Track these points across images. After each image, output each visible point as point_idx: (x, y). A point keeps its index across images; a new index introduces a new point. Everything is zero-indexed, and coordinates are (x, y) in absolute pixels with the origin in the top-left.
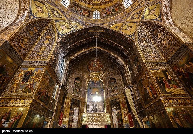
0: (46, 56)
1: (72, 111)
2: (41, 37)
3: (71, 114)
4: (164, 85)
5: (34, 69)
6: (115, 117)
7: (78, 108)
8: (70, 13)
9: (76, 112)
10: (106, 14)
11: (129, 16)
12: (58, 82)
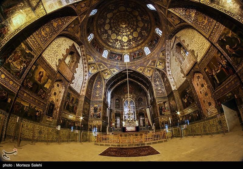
0: (100, 97)
1: (116, 119)
2: (95, 83)
3: (116, 121)
4: (162, 110)
5: (97, 106)
6: (141, 122)
7: (119, 118)
8: (109, 62)
9: (118, 120)
10: (133, 57)
11: (148, 63)
12: (108, 107)
